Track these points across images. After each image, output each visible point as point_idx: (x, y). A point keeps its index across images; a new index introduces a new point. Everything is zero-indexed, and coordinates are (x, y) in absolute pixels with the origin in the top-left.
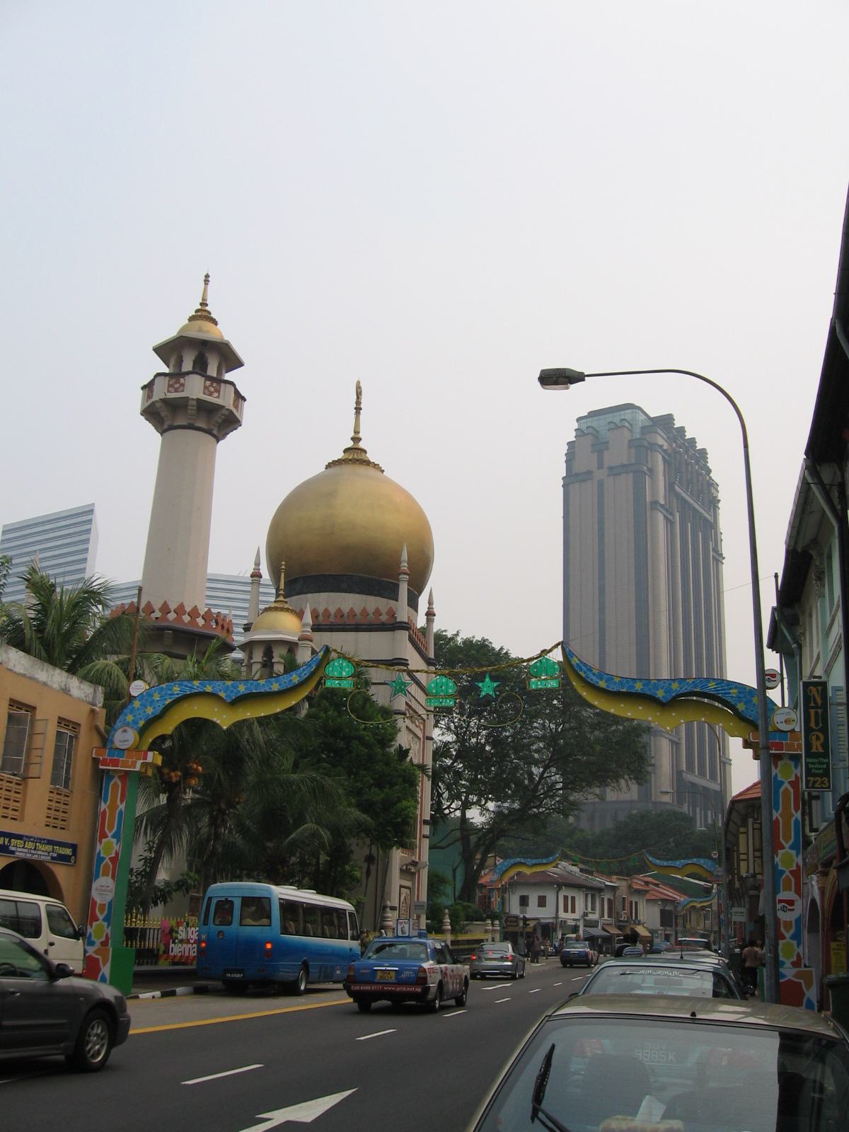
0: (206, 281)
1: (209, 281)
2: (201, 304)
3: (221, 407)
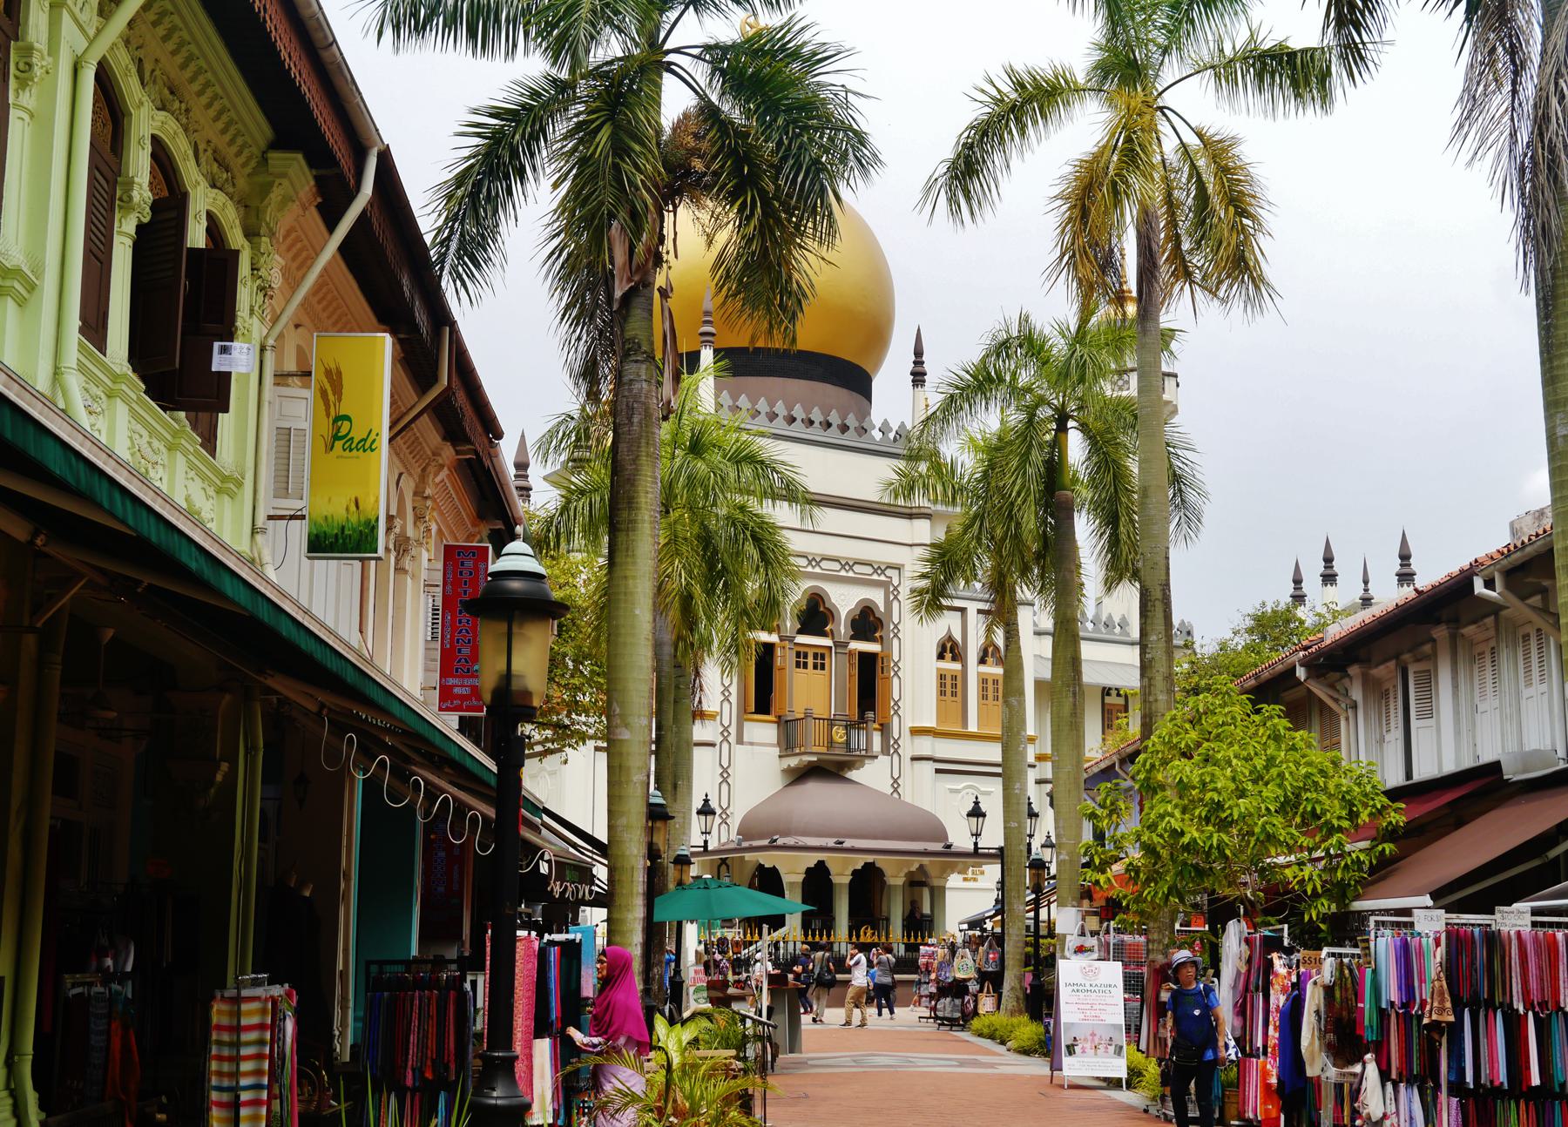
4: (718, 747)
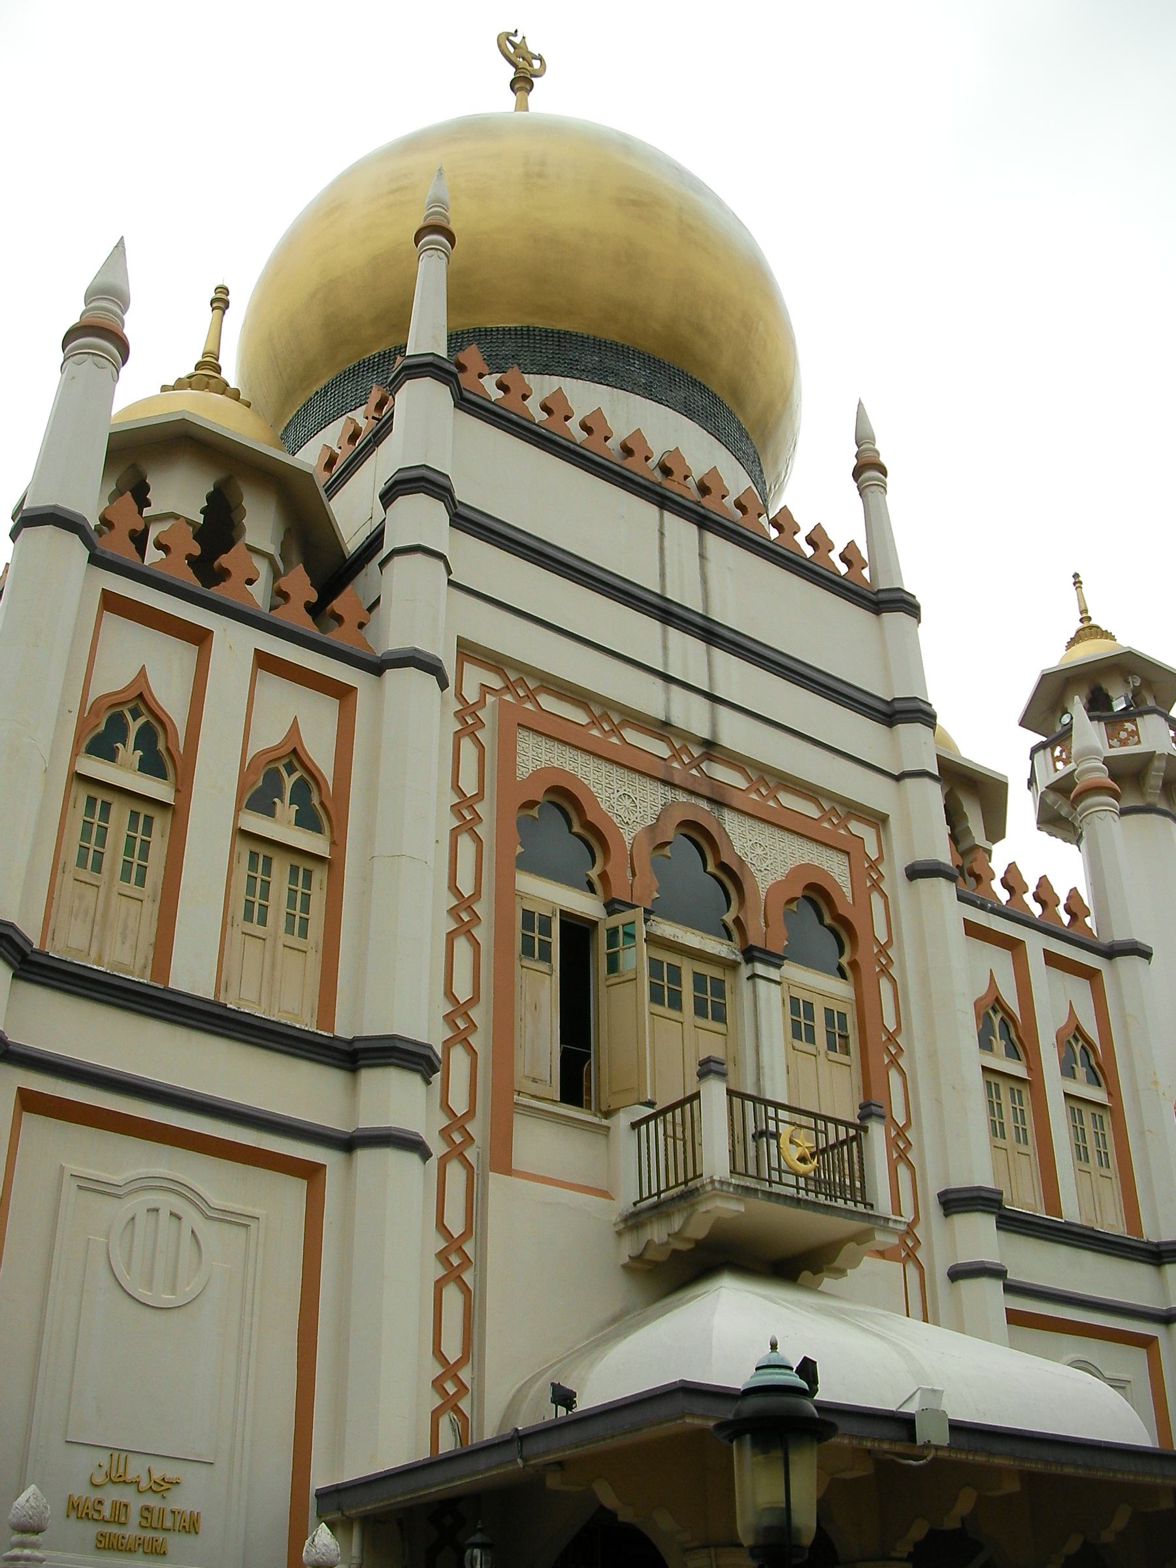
0: (1077, 582)
1: (1081, 583)
2: (1081, 620)
3: (1150, 757)
4: (433, 1162)
